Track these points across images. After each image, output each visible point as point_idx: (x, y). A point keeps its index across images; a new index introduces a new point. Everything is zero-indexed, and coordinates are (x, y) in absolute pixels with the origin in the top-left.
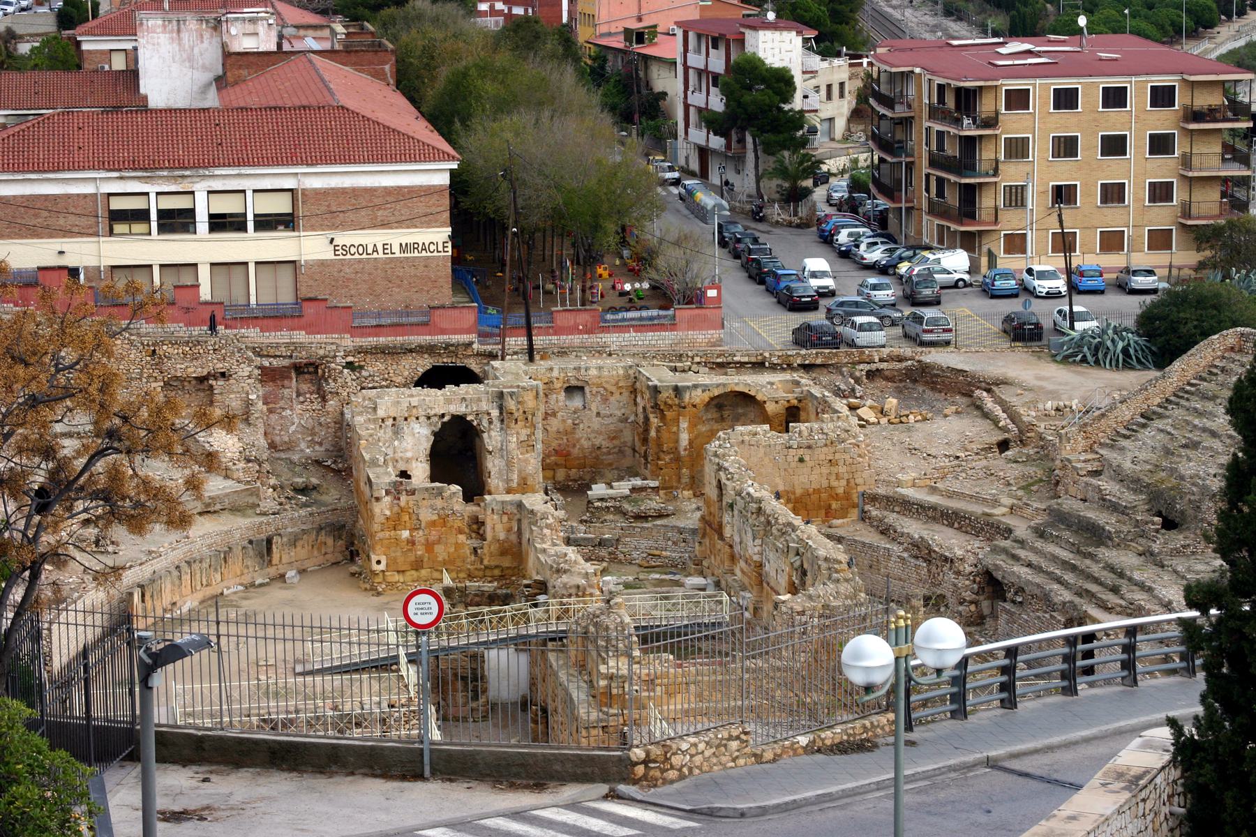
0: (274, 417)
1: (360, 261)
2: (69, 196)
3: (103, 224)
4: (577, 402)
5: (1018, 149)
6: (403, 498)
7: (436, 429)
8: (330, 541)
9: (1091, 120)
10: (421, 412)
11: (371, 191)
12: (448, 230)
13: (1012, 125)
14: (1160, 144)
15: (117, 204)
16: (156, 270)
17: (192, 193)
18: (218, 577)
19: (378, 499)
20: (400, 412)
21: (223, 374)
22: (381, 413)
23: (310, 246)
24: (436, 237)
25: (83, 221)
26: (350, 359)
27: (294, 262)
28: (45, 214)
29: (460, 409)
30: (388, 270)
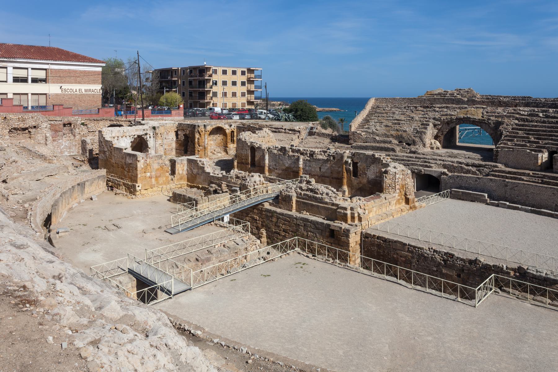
1: (70, 94)
5: (215, 83)
6: (148, 160)
7: (133, 140)
8: (102, 183)
9: (229, 78)
10: (127, 134)
11: (75, 71)
14: (243, 84)
17: (6, 68)
19: (139, 161)
20: (120, 135)
22: (113, 135)
23: (52, 89)
24: (97, 88)
26: (83, 122)
27: (46, 94)
29: (141, 133)
30: (81, 97)
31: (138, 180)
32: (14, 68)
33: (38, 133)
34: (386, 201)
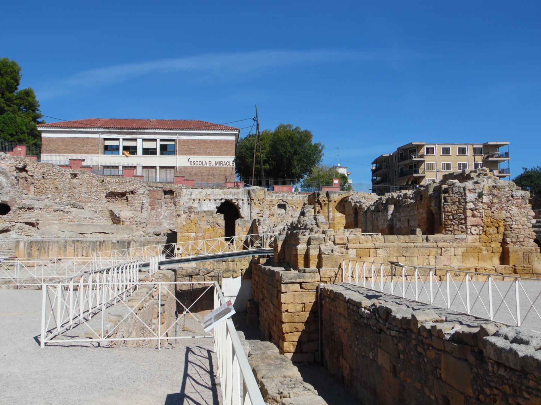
0: (154, 212)
1: (200, 168)
2: (88, 138)
3: (102, 148)
4: (282, 211)
6: (193, 216)
7: (219, 206)
10: (212, 197)
12: (233, 158)
13: (429, 159)
15: (107, 143)
16: (121, 168)
18: (95, 254)
21: (132, 192)
22: (193, 197)
23: (179, 161)
24: (229, 160)
25: (93, 148)
28: (79, 145)
29: (229, 197)
31: (178, 240)
32: (144, 140)
33: (135, 200)
34: (428, 244)
